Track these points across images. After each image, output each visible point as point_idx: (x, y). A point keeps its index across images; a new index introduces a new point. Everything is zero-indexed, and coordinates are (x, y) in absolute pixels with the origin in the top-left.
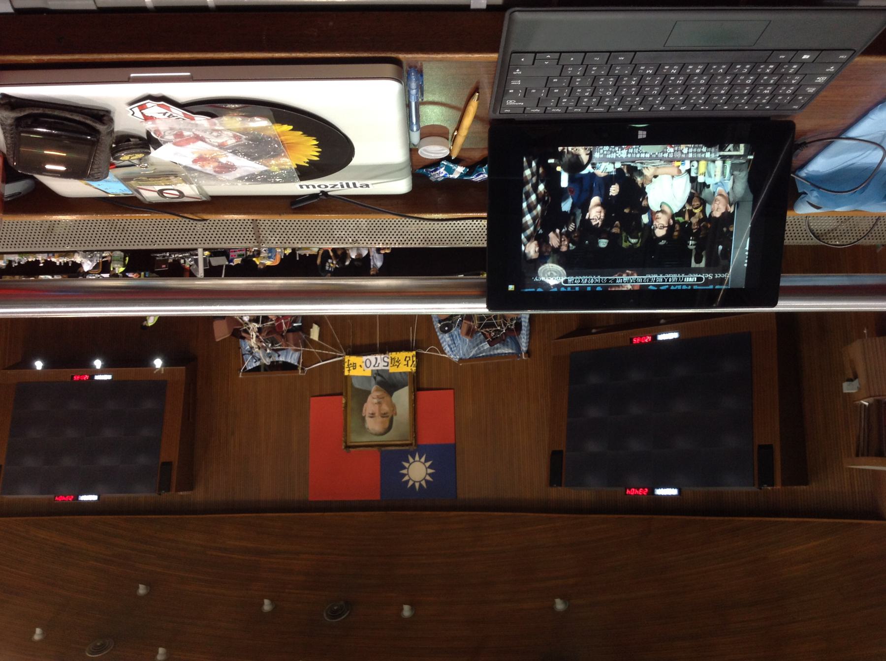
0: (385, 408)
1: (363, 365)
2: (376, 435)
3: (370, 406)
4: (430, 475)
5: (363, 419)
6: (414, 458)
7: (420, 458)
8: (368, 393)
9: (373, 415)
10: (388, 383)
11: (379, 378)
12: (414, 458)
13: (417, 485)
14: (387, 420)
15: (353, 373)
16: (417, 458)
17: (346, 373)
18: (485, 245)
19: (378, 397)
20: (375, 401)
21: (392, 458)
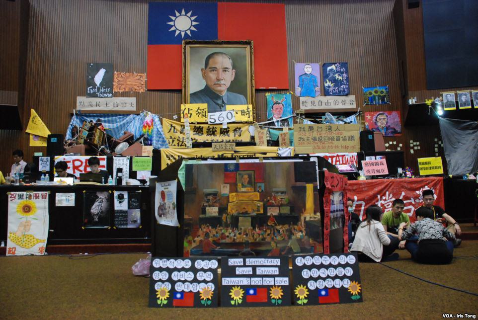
0: (213, 75)
1: (234, 113)
2: (222, 53)
3: (228, 78)
4: (172, 20)
5: (234, 67)
6: (186, 34)
7: (180, 34)
8: (229, 90)
9: (225, 70)
10: (210, 96)
11: (220, 102)
12: (186, 34)
13: (183, 12)
14: (211, 64)
15: (244, 107)
16: (183, 34)
17: (250, 106)
18: (74, 205)
19: (220, 85)
20: (222, 82)
21: (204, 36)
